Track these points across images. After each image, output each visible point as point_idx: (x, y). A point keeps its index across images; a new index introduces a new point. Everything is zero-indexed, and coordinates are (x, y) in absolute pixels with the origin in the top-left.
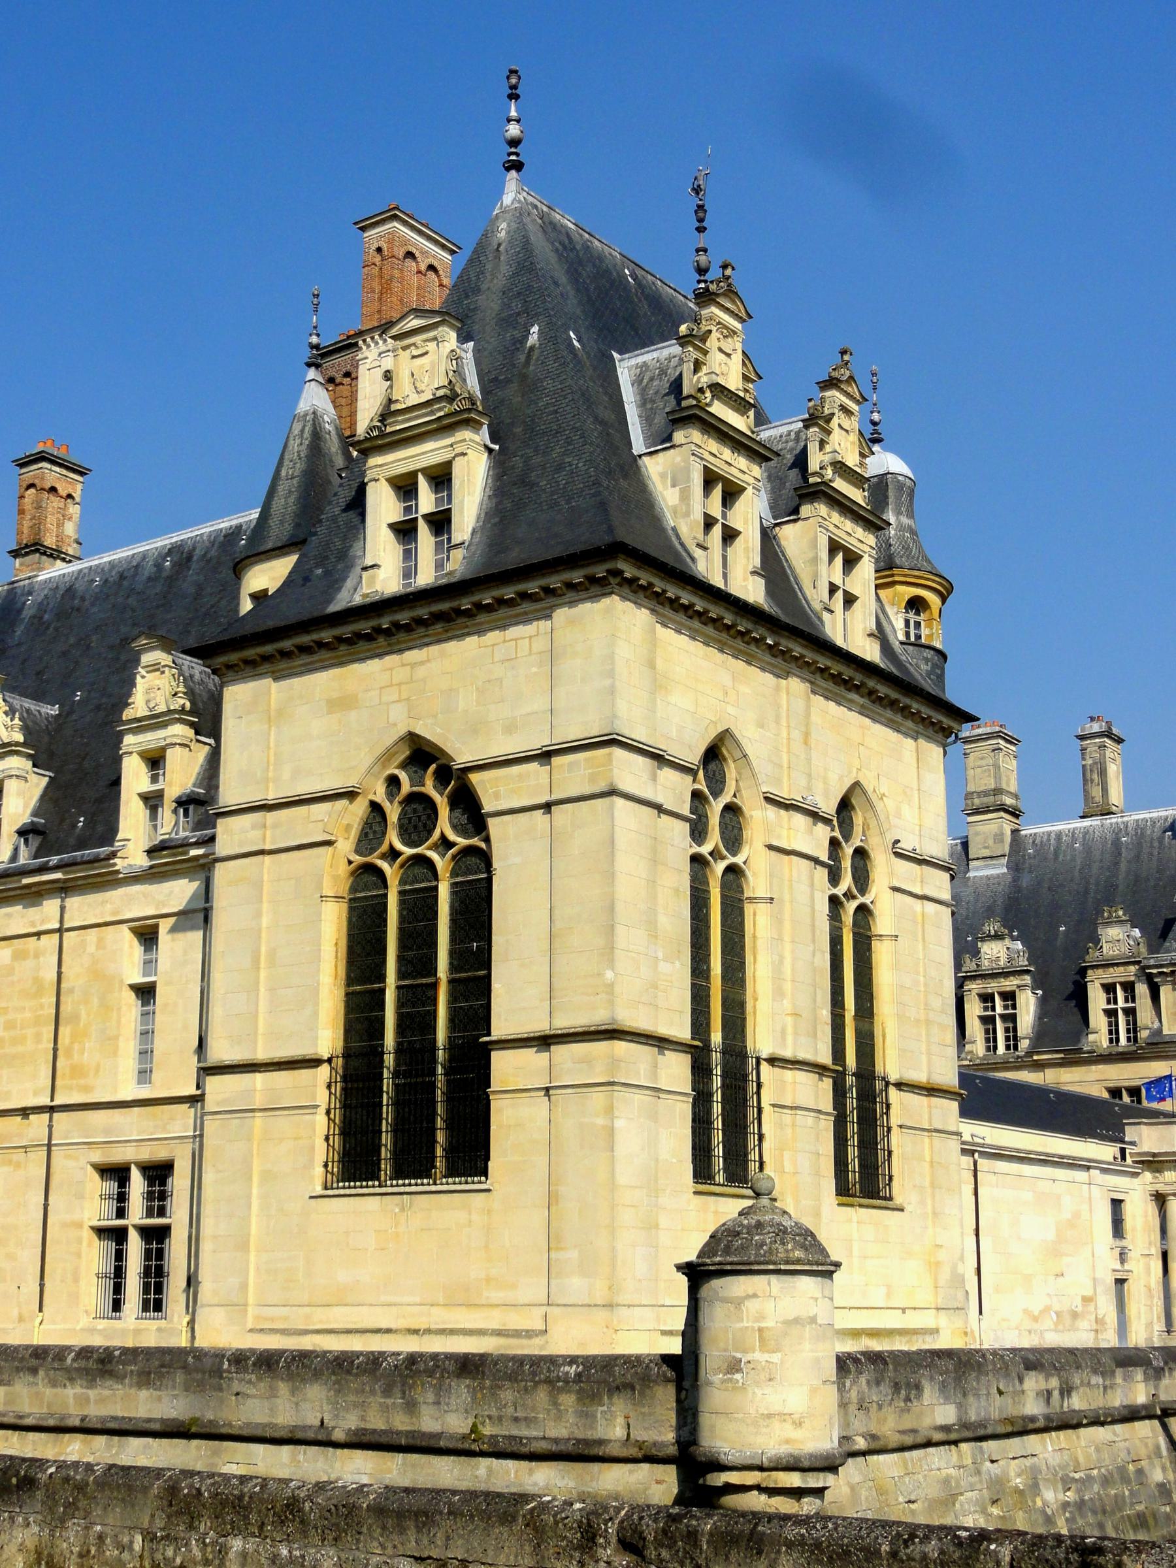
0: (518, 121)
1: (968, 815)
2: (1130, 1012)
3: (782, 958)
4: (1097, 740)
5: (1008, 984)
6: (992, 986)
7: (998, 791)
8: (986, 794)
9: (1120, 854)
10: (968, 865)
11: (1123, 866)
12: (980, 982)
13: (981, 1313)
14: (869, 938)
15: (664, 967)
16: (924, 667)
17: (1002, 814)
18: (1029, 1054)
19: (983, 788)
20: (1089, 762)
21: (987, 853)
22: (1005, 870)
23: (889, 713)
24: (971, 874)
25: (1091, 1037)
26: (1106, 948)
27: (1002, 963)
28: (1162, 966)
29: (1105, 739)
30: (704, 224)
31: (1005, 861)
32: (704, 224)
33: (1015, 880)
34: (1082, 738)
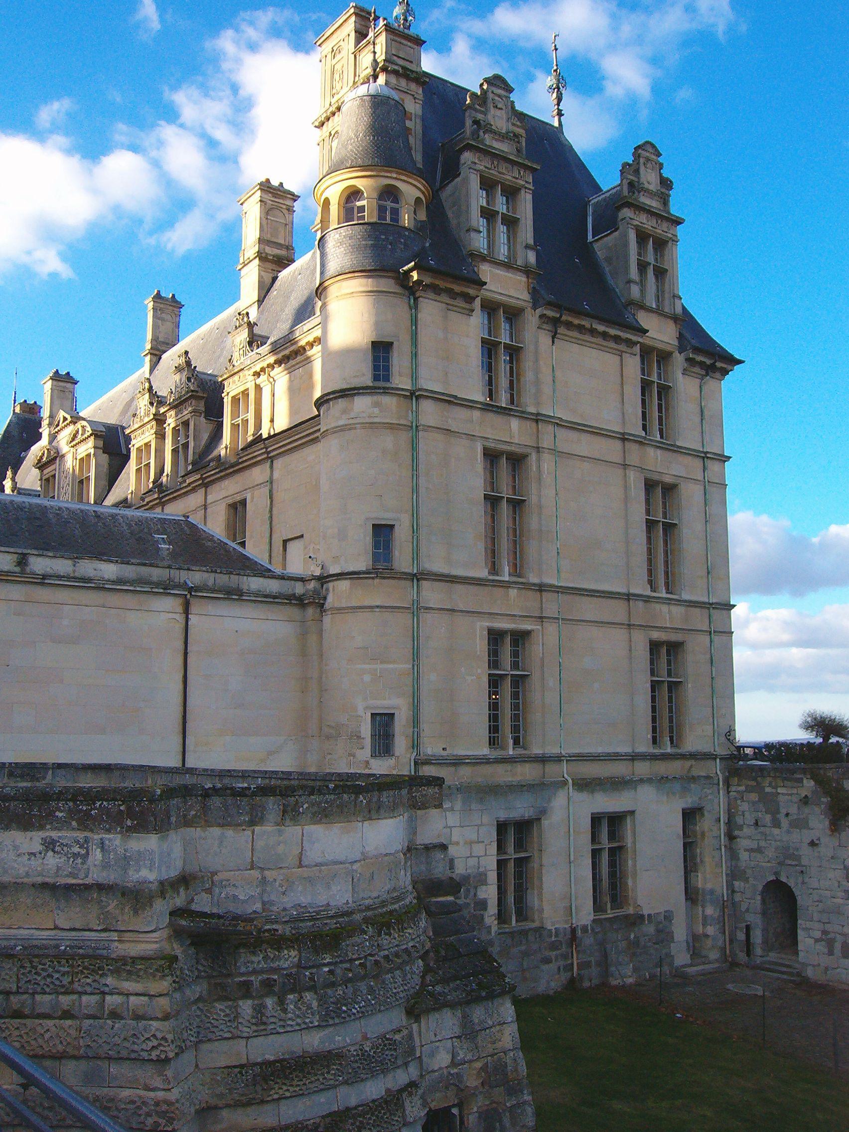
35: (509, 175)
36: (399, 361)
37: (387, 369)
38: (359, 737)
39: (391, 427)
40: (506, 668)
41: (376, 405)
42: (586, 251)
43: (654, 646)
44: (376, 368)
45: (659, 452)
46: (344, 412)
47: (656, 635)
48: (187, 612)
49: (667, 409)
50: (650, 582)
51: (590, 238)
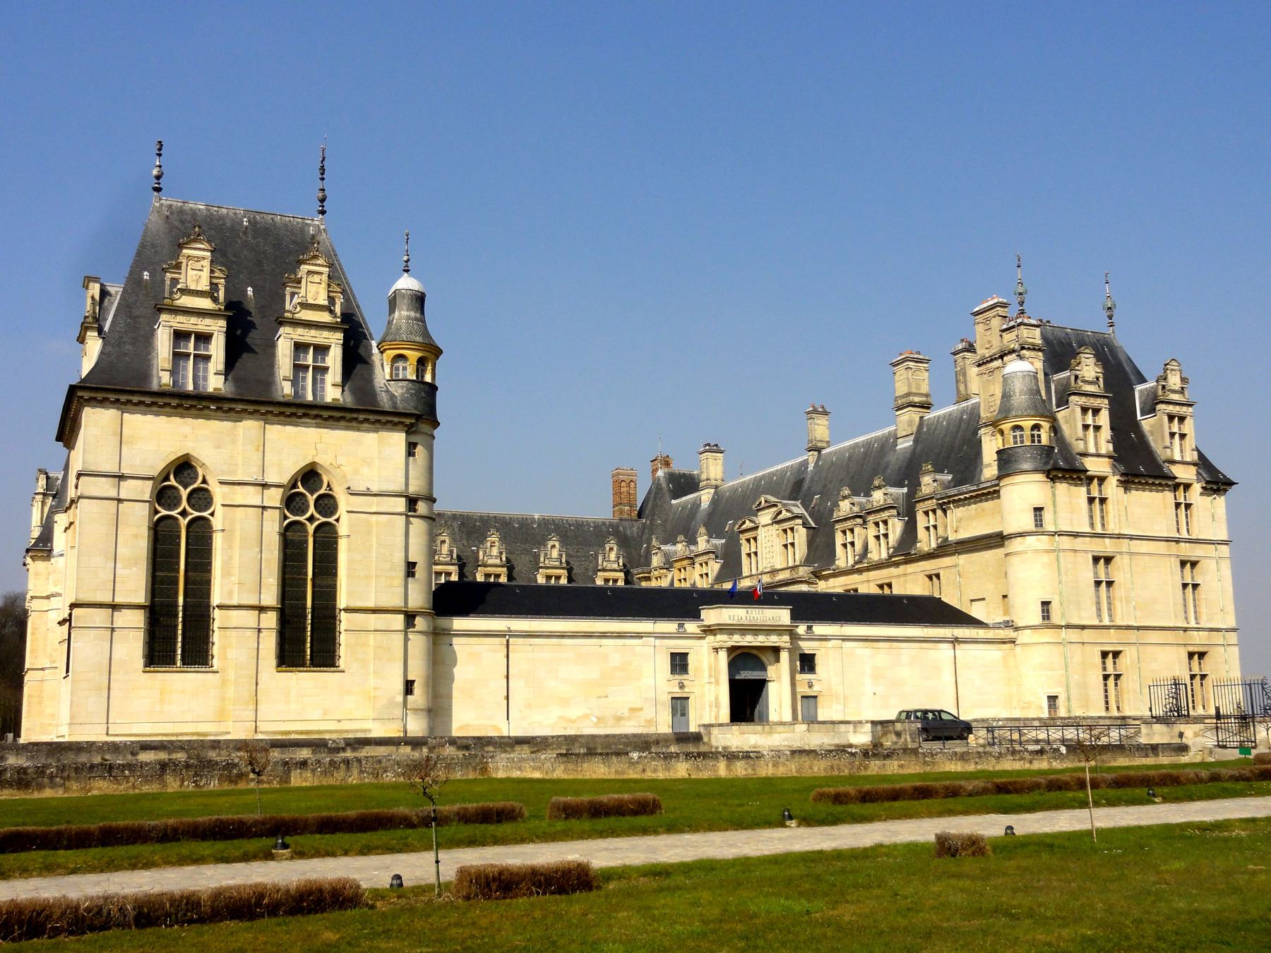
0: (160, 166)
1: (897, 410)
2: (935, 527)
3: (230, 558)
5: (885, 515)
7: (908, 394)
9: (960, 426)
11: (960, 435)
13: (508, 719)
14: (336, 538)
15: (127, 572)
16: (400, 391)
17: (910, 408)
18: (890, 557)
20: (959, 369)
22: (911, 443)
23: (343, 423)
24: (898, 448)
25: (918, 545)
26: (923, 488)
28: (942, 498)
29: (966, 353)
30: (324, 176)
31: (912, 438)
32: (324, 176)
33: (915, 449)
34: (954, 354)
35: (1096, 402)
36: (1047, 516)
37: (1041, 520)
38: (1042, 708)
39: (1047, 551)
40: (1110, 670)
41: (1038, 540)
42: (1136, 426)
43: (1191, 655)
44: (1036, 520)
45: (1187, 544)
46: (1020, 544)
47: (1191, 649)
48: (954, 649)
49: (1191, 516)
50: (1186, 618)
51: (1139, 417)
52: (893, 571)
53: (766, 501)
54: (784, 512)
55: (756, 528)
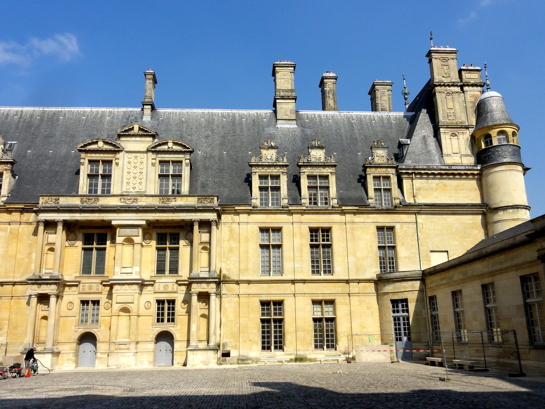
4: (332, 80)
6: (317, 172)
8: (287, 91)
10: (276, 122)
12: (309, 169)
19: (285, 88)
21: (287, 117)
27: (322, 161)
28: (408, 169)
52: (337, 218)
53: (140, 129)
54: (170, 145)
55: (117, 150)
